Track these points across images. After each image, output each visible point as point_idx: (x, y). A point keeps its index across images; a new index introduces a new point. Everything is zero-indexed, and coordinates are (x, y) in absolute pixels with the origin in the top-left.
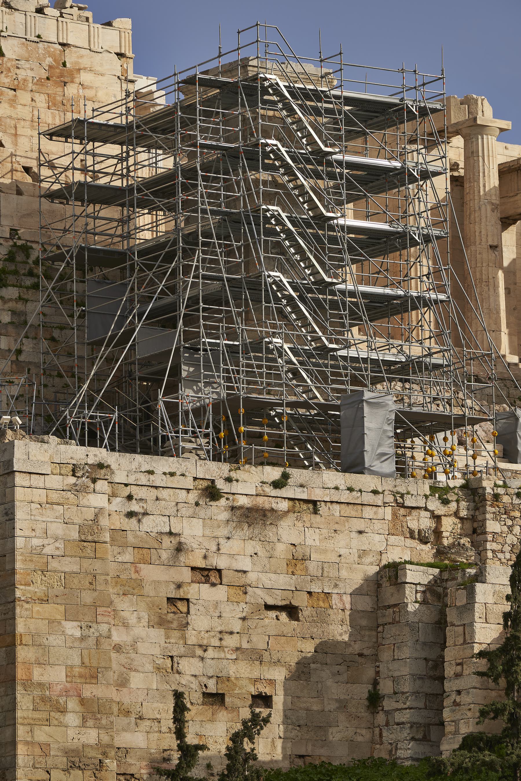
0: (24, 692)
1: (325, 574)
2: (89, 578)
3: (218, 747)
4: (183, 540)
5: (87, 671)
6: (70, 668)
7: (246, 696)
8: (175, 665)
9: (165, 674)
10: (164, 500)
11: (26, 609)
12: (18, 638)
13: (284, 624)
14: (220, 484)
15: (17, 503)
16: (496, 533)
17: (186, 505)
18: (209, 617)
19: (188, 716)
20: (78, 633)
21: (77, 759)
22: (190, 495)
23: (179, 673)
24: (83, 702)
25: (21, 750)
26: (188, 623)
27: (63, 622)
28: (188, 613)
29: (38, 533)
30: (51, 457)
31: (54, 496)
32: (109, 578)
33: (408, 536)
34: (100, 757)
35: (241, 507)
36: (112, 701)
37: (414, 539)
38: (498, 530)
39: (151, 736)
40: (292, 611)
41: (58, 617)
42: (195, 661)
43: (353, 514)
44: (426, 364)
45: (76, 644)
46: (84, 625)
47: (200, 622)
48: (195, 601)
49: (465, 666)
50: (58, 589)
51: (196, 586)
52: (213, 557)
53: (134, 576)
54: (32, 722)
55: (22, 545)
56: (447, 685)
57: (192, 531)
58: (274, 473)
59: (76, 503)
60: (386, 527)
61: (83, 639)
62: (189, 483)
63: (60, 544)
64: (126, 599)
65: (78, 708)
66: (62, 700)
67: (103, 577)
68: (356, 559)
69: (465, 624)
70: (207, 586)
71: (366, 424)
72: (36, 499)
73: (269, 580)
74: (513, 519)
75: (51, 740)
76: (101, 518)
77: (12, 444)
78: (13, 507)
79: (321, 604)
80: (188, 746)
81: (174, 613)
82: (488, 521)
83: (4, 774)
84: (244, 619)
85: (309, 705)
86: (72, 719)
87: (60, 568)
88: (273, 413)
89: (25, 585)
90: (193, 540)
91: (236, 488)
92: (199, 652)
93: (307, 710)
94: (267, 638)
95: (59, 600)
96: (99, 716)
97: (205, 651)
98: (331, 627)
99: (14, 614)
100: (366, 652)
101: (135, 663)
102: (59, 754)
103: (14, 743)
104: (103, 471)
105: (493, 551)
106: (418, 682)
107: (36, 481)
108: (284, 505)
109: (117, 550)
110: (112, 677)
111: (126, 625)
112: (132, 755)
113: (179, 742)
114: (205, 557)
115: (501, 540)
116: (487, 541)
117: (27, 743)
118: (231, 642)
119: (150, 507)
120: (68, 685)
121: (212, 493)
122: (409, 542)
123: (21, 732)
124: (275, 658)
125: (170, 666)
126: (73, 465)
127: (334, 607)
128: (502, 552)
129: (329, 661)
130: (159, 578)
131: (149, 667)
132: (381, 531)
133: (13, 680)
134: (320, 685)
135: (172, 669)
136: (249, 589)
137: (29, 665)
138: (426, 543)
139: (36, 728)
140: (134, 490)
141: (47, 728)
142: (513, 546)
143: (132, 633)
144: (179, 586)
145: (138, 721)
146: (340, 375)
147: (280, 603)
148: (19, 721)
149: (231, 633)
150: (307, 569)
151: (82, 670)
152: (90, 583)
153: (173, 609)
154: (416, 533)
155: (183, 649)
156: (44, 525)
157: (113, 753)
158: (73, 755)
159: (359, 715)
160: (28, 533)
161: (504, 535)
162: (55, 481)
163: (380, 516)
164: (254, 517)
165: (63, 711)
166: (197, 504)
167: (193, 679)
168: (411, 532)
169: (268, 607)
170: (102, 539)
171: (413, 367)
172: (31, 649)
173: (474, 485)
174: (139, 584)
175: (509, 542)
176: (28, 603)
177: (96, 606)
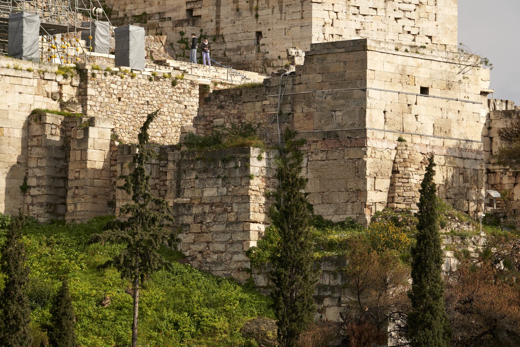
33: (46, 95)
38: (94, 94)
43: (17, 82)
49: (81, 174)
56: (70, 183)
68: (17, 108)
69: (81, 150)
82: (88, 89)
98: (3, 147)
105: (91, 106)
106: (51, 180)
115: (95, 99)
128: (95, 106)
138: (55, 100)
142: (101, 103)
154: (50, 95)
159: (16, 197)
163: (31, 84)
168: (48, 94)
173: (81, 67)
175: (99, 101)
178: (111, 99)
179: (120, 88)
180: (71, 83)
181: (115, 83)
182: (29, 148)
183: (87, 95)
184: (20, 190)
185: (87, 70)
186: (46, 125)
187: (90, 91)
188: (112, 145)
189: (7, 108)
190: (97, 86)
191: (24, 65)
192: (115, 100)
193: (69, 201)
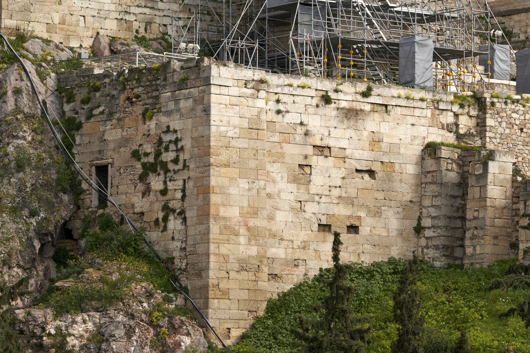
0: (214, 223)
1: (392, 150)
2: (254, 152)
3: (327, 258)
4: (308, 128)
5: (252, 210)
6: (242, 208)
7: (344, 226)
8: (303, 206)
9: (297, 212)
10: (298, 103)
11: (217, 171)
12: (211, 189)
13: (367, 182)
14: (333, 95)
15: (212, 105)
16: (492, 126)
17: (311, 107)
18: (323, 177)
19: (341, 247)
20: (247, 186)
21: (245, 265)
22: (313, 100)
23: (304, 211)
24: (249, 229)
25: (212, 258)
26: (310, 181)
27: (238, 179)
28: (311, 174)
29: (224, 123)
30: (232, 75)
31: (234, 100)
32: (265, 152)
34: (259, 264)
35: (343, 109)
36: (266, 228)
37: (444, 129)
38: (493, 125)
39: (288, 250)
40: (371, 173)
41: (235, 176)
42: (315, 205)
43: (409, 113)
44: (445, 17)
45: (246, 193)
46: (250, 181)
47: (318, 181)
48: (315, 167)
50: (235, 158)
51: (315, 157)
52: (326, 139)
53: (280, 150)
54: (219, 241)
55: (215, 131)
56: (468, 224)
57: (314, 123)
58: (362, 87)
59: (247, 105)
60: (427, 121)
61: (249, 190)
62: (313, 93)
63: (237, 130)
64: (275, 165)
65: (246, 233)
66: (237, 228)
67: (262, 151)
68: (410, 141)
69: (480, 186)
70: (322, 157)
71: (416, 57)
72: (223, 102)
73: (357, 154)
74: (502, 117)
75: (230, 252)
76: (261, 115)
77: (209, 67)
78: (210, 106)
79: (389, 169)
80: (341, 266)
81: (302, 174)
82: (487, 119)
83: (200, 273)
84: (343, 178)
85: (380, 232)
86: (242, 240)
87: (237, 146)
88: (355, 47)
89: (216, 156)
90: (314, 129)
91: (340, 96)
92: (317, 198)
93: (379, 236)
94: (357, 190)
95: (236, 165)
96: (258, 238)
97: (321, 198)
98: (394, 184)
99: (209, 174)
100: (414, 200)
101: (279, 205)
102: (235, 261)
103: (208, 255)
104: (263, 85)
105: (490, 138)
106: (447, 220)
107: (224, 90)
108: (368, 108)
109: (270, 134)
110: (265, 213)
111: (274, 182)
112: (276, 262)
113: (335, 263)
114: (322, 139)
115: (494, 131)
116: (486, 131)
117: (216, 254)
118: (336, 192)
119: (289, 107)
120: (241, 219)
121: (327, 100)
122: (441, 132)
123: (212, 248)
124: (361, 203)
125: (299, 207)
126: (246, 80)
127: (396, 171)
128: (495, 138)
129: (392, 206)
130: (294, 152)
131: (287, 208)
132: (424, 124)
133: (208, 215)
134: (387, 220)
135: (301, 209)
136: (347, 160)
137: (217, 206)
138: (451, 132)
139: (221, 245)
140: (281, 97)
141: (227, 245)
142: (502, 134)
143: (277, 186)
144: (306, 157)
145: (280, 241)
146: (396, 23)
147: (365, 169)
148: (211, 240)
149: (336, 187)
150: (380, 147)
151: (249, 210)
152: (254, 155)
153: (302, 172)
154: (445, 126)
155: (307, 197)
156: (227, 118)
157: (265, 262)
158: (242, 262)
159: (410, 239)
160: (218, 123)
161: (496, 128)
162: (234, 91)
163: (424, 115)
164: (351, 114)
165: (237, 235)
166: (317, 106)
167: (313, 216)
168: (443, 125)
169: (358, 171)
170: (261, 128)
171: (438, 18)
172: (219, 195)
173: (479, 96)
174: (282, 155)
175: (499, 132)
176: (217, 167)
177: (257, 170)
178: (512, 131)
179: (522, 118)
180: (468, 113)
181: (516, 112)
182: (423, 185)
183: (485, 126)
184: (413, 231)
185: (485, 98)
186: (442, 159)
187: (490, 122)
188: (514, 181)
189: (398, 142)
190: (497, 116)
191: (417, 94)
192: (517, 131)
193: (467, 243)
